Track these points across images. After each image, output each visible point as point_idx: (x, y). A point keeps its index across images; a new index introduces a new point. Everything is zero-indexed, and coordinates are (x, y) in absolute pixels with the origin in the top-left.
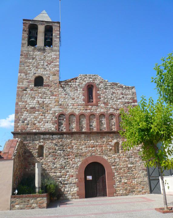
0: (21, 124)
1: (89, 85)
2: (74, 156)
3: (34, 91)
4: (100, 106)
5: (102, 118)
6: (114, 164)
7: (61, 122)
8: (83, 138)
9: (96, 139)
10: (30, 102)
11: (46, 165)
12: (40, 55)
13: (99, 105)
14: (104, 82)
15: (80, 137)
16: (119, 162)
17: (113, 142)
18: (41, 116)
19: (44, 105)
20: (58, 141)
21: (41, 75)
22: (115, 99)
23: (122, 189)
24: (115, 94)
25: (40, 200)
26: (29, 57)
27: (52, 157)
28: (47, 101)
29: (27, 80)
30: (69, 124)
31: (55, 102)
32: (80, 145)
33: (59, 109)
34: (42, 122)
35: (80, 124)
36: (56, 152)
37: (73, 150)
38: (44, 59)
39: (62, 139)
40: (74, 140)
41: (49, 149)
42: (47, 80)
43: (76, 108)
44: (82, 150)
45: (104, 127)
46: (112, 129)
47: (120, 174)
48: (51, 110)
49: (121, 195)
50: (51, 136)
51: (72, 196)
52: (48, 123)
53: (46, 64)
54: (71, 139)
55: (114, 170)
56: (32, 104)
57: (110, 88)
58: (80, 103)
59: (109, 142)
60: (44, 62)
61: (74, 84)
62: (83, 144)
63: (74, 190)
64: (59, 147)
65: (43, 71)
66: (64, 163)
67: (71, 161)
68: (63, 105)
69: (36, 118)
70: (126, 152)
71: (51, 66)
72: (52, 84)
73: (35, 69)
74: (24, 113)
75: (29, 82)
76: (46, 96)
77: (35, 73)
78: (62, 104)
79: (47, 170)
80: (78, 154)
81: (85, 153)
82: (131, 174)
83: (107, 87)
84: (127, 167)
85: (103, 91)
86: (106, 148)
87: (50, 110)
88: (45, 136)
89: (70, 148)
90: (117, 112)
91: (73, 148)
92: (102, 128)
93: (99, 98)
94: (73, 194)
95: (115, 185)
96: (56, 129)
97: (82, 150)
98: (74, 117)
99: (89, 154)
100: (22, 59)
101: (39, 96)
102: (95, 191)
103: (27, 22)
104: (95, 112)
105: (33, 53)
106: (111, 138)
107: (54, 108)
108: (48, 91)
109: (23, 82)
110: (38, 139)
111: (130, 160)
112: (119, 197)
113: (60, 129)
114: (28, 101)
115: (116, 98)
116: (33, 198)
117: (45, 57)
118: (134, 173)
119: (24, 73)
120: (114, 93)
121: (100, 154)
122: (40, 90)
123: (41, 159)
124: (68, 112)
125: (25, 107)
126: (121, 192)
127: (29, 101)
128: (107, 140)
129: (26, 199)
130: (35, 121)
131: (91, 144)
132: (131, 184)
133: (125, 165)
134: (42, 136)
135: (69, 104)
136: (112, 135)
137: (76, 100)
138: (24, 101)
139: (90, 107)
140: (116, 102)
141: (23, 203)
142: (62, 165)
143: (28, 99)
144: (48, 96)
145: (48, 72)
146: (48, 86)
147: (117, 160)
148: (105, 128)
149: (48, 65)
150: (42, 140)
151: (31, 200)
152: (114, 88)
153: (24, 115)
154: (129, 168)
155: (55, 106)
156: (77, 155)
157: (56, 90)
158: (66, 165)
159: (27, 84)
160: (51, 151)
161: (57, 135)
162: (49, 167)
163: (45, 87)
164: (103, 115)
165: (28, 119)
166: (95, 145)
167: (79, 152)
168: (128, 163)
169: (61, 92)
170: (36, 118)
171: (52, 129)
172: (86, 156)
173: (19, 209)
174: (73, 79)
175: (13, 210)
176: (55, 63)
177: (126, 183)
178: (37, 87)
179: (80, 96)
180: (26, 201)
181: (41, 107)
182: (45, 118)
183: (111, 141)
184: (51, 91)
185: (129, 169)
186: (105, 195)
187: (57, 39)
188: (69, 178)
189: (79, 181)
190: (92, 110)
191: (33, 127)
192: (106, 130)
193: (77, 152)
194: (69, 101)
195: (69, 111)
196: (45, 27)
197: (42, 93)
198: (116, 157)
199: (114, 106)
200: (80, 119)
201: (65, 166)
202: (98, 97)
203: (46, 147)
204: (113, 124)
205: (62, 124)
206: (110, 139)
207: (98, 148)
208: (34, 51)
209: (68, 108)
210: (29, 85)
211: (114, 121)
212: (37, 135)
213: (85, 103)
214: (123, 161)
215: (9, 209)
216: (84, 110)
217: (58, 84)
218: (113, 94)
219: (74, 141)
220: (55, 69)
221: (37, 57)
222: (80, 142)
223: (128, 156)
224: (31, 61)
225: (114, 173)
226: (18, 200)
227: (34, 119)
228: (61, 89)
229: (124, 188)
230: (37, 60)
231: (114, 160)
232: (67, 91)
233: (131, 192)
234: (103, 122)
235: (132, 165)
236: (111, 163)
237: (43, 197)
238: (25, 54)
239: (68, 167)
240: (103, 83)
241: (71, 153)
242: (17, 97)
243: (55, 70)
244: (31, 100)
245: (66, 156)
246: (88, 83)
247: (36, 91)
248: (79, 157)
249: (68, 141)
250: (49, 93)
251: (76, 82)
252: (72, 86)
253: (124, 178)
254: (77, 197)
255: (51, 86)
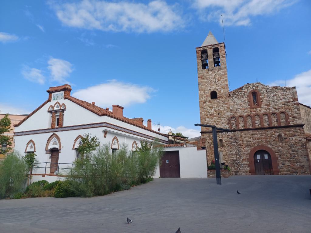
21: (214, 90)
22: (276, 100)
28: (221, 109)
52: (223, 124)
53: (217, 81)
62: (250, 137)
77: (210, 90)
101: (215, 106)
126: (285, 172)
159: (206, 98)
177: (289, 166)
184: (223, 101)
202: (261, 101)
252: (239, 95)
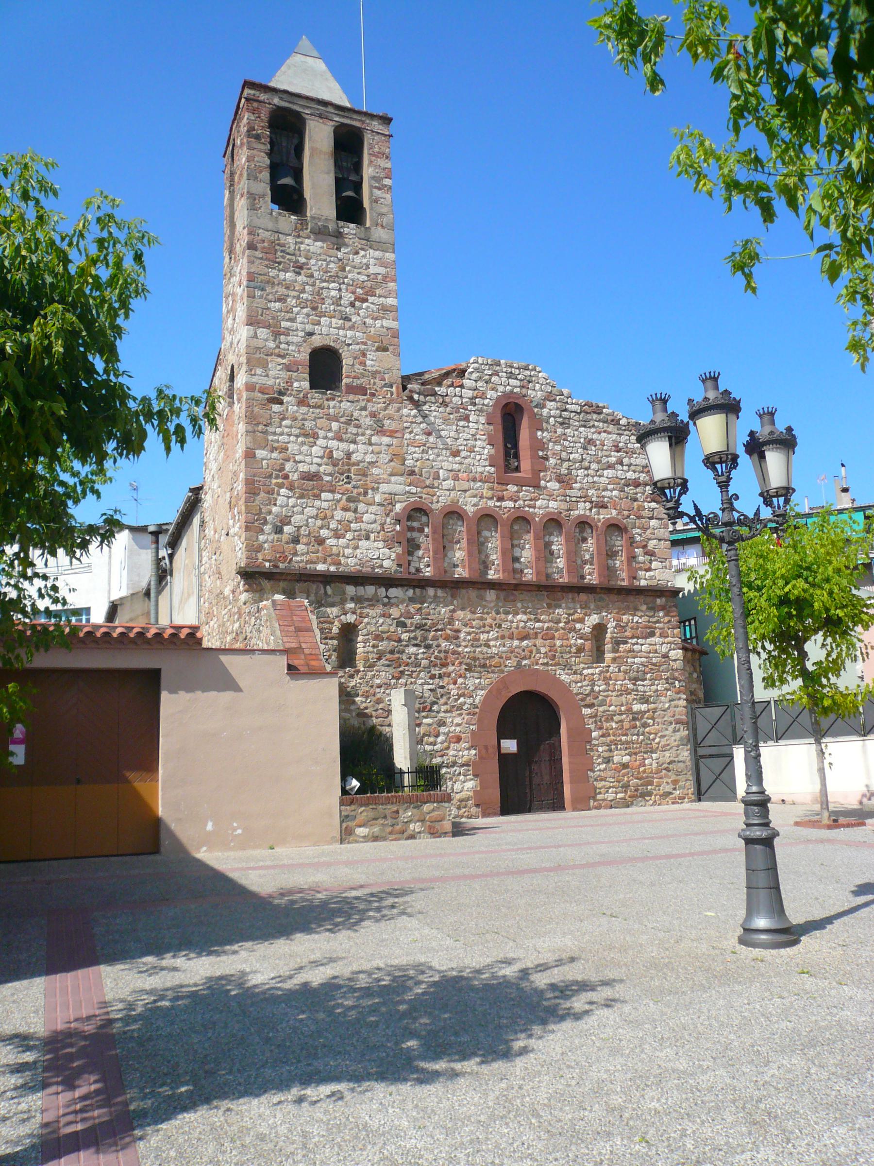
0: (270, 538)
1: (507, 404)
2: (464, 667)
3: (314, 407)
4: (546, 487)
5: (551, 534)
6: (591, 699)
7: (413, 540)
8: (491, 602)
9: (534, 608)
10: (300, 453)
11: (367, 697)
12: (323, 257)
13: (543, 483)
14: (558, 398)
15: (481, 598)
16: (606, 694)
17: (588, 623)
18: (345, 509)
19: (353, 469)
20: (408, 612)
21: (332, 344)
22: (594, 466)
23: (613, 787)
24: (593, 448)
25: (433, 810)
26: (283, 257)
27: (387, 669)
28: (360, 452)
29: (280, 360)
30: (444, 547)
31: (391, 461)
32: (482, 629)
33: (407, 488)
34: (349, 535)
35: (480, 552)
36: (403, 652)
37: (459, 646)
38: (340, 274)
39: (422, 603)
40: (463, 609)
41: (378, 637)
42: (359, 368)
43: (465, 491)
44: (489, 646)
45: (558, 567)
46: (583, 577)
47: (609, 736)
48: (378, 488)
49: (611, 807)
50: (382, 591)
51: (459, 808)
52: (367, 538)
53: (347, 297)
54: (452, 604)
55: (590, 722)
56: (308, 459)
57: (577, 423)
58: (480, 469)
59: (573, 621)
60: (340, 290)
61: (456, 395)
62: (491, 626)
63: (465, 788)
64: (412, 631)
65: (338, 328)
66: (431, 690)
67: (452, 686)
68: (421, 475)
69: (325, 518)
70: (627, 662)
71: (368, 307)
72: (374, 384)
73: (308, 315)
74: (278, 494)
75: (288, 368)
76: (357, 434)
77: (311, 334)
78: (416, 469)
79: (371, 716)
80: (475, 659)
81: (497, 659)
82: (641, 737)
83: (569, 418)
84: (629, 710)
85: (556, 432)
86: (565, 642)
87: (373, 489)
88: (361, 591)
89: (447, 638)
90: (599, 514)
91: (457, 638)
92: (550, 571)
93: (542, 458)
94: (461, 801)
95: (594, 772)
96: (399, 565)
97: (489, 646)
98: (460, 523)
99: (511, 663)
100: (253, 262)
101: (330, 430)
102: (528, 791)
103: (263, 97)
104: (531, 510)
105: (296, 243)
106: (581, 608)
107: (389, 482)
108: (364, 413)
109: (265, 366)
110: (337, 599)
111: (639, 688)
112: (602, 811)
113: (413, 564)
114: (293, 448)
115: (599, 462)
116: (411, 803)
117: (343, 269)
118: (650, 733)
119: (268, 327)
120: (590, 442)
121: (547, 664)
122: (332, 404)
123: (352, 676)
124: (438, 502)
125: (282, 469)
126: (610, 796)
127: (296, 447)
128: (569, 615)
129: (389, 807)
130: (321, 528)
131: (517, 628)
132: (642, 769)
133: (622, 705)
134: (350, 590)
135: (441, 471)
136: (583, 596)
137: (465, 458)
138: (276, 445)
139: (512, 488)
140: (596, 479)
141: (381, 821)
142: (422, 700)
143: (292, 438)
144: (363, 435)
145: (358, 334)
146: (362, 390)
147: (600, 687)
148: (560, 571)
149: (357, 304)
150: (352, 605)
151: (405, 810)
152: (591, 424)
153: (278, 503)
154: (636, 716)
155: (391, 475)
156: (475, 665)
157: (391, 411)
158: (438, 699)
159: (284, 375)
160: (383, 645)
161: (402, 586)
162: (378, 703)
163: (351, 397)
164: (554, 524)
165: (297, 519)
166: (531, 632)
167: (481, 652)
168: (634, 699)
169: (412, 423)
170: (325, 518)
171: (386, 563)
172: (502, 667)
173: (366, 839)
174: (447, 374)
175: (349, 843)
176: (382, 299)
177: (625, 766)
178: (323, 393)
179: (479, 443)
180: (388, 812)
181: (342, 474)
182: (358, 520)
183: (581, 621)
184: (373, 415)
185: (634, 719)
186: (557, 805)
187: (384, 195)
188: (446, 744)
189: (481, 758)
190: (521, 502)
191: (318, 552)
192: (564, 579)
193: (472, 655)
194: (442, 461)
195: (441, 500)
196: (335, 132)
197: (342, 420)
198: (596, 677)
199: (591, 492)
200: (479, 533)
201: (435, 703)
202: (541, 453)
203: (365, 631)
204: (587, 557)
205: (418, 547)
206: (579, 611)
207: (539, 642)
208: (299, 236)
209: (438, 488)
210: (289, 382)
211: (590, 545)
212: (333, 585)
213: (497, 472)
214: (618, 691)
215: (337, 841)
216: (491, 498)
217: (397, 388)
218: (589, 447)
219: (460, 614)
220: (386, 323)
221: (313, 262)
222: (481, 619)
223: (633, 674)
224: (289, 275)
225: (591, 731)
226: (363, 813)
227: (319, 523)
228: (408, 411)
229: (619, 782)
230: (312, 276)
231: (589, 688)
232: (432, 419)
233: (640, 797)
234: (554, 547)
235: (644, 707)
236: (580, 697)
237: (441, 802)
238: (263, 241)
239: (443, 708)
240: (554, 400)
241: (452, 657)
242: (250, 428)
243: (382, 326)
244: (303, 444)
245: (435, 666)
246: (505, 395)
247: (319, 407)
248: (480, 672)
249: (443, 611)
250: (368, 421)
251: (462, 386)
252: (447, 399)
253: (621, 749)
254: (474, 810)
255: (373, 395)
